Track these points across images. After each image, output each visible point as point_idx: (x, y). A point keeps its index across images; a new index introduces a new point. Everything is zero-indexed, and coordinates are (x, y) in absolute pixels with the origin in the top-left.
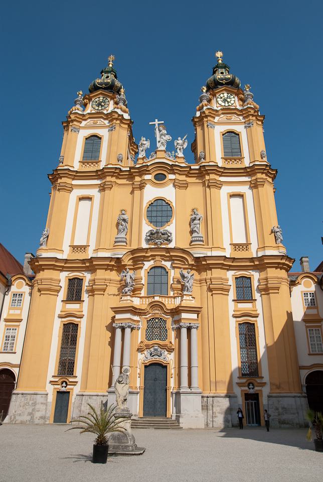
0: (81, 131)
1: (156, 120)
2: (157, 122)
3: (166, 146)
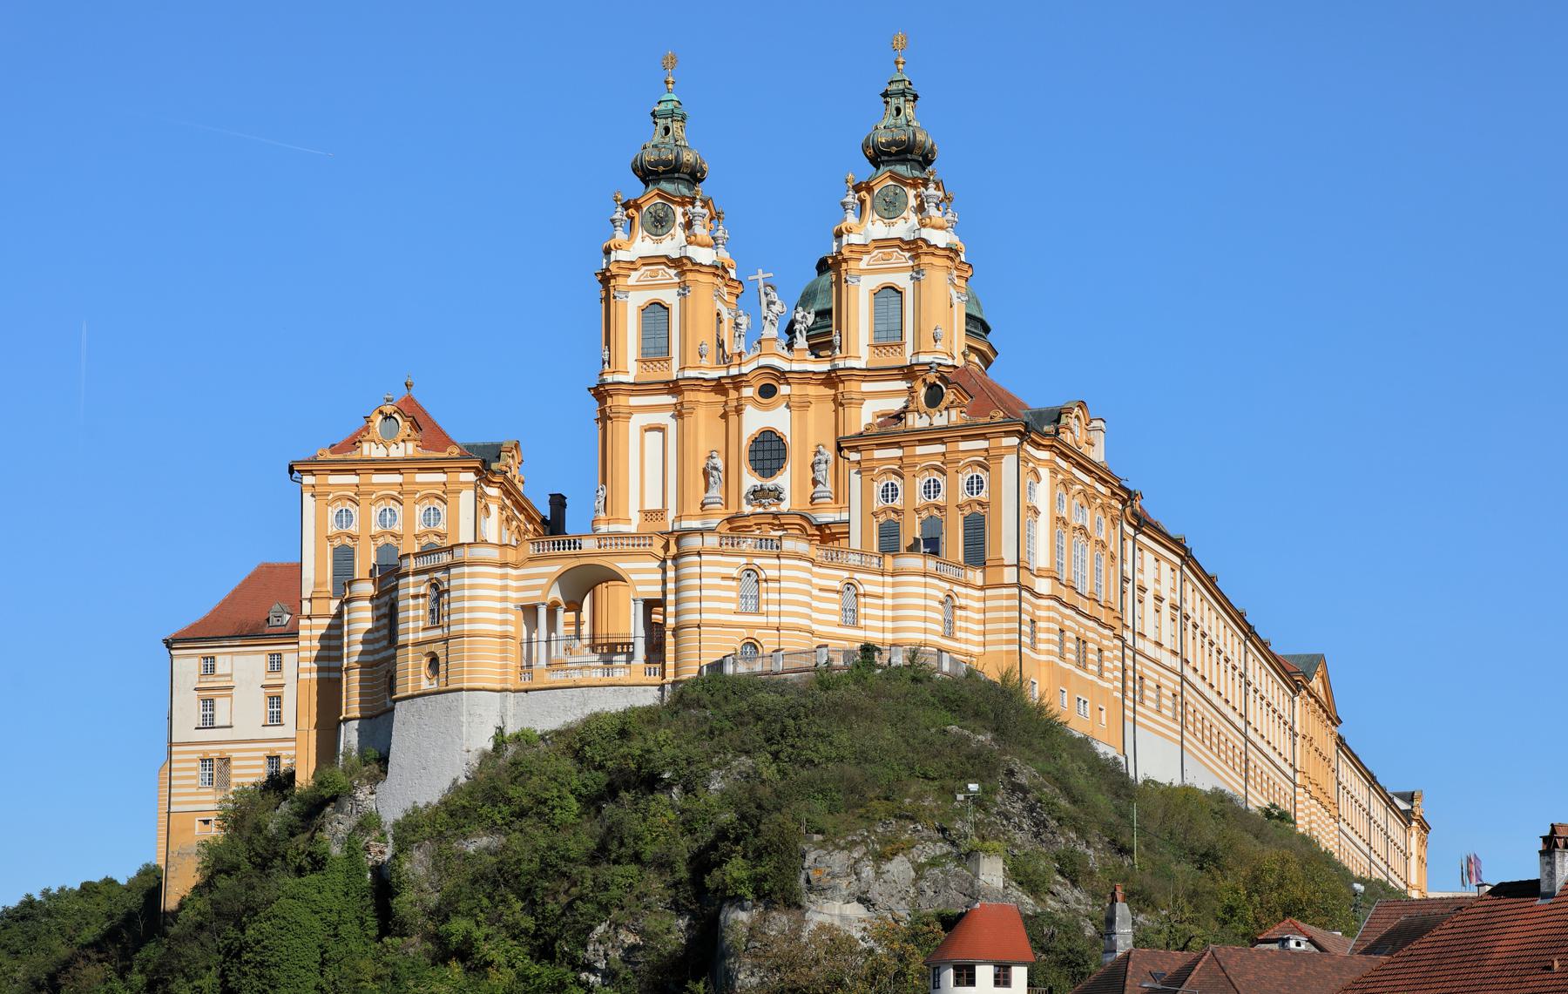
1: (760, 271)
2: (761, 275)
3: (777, 325)
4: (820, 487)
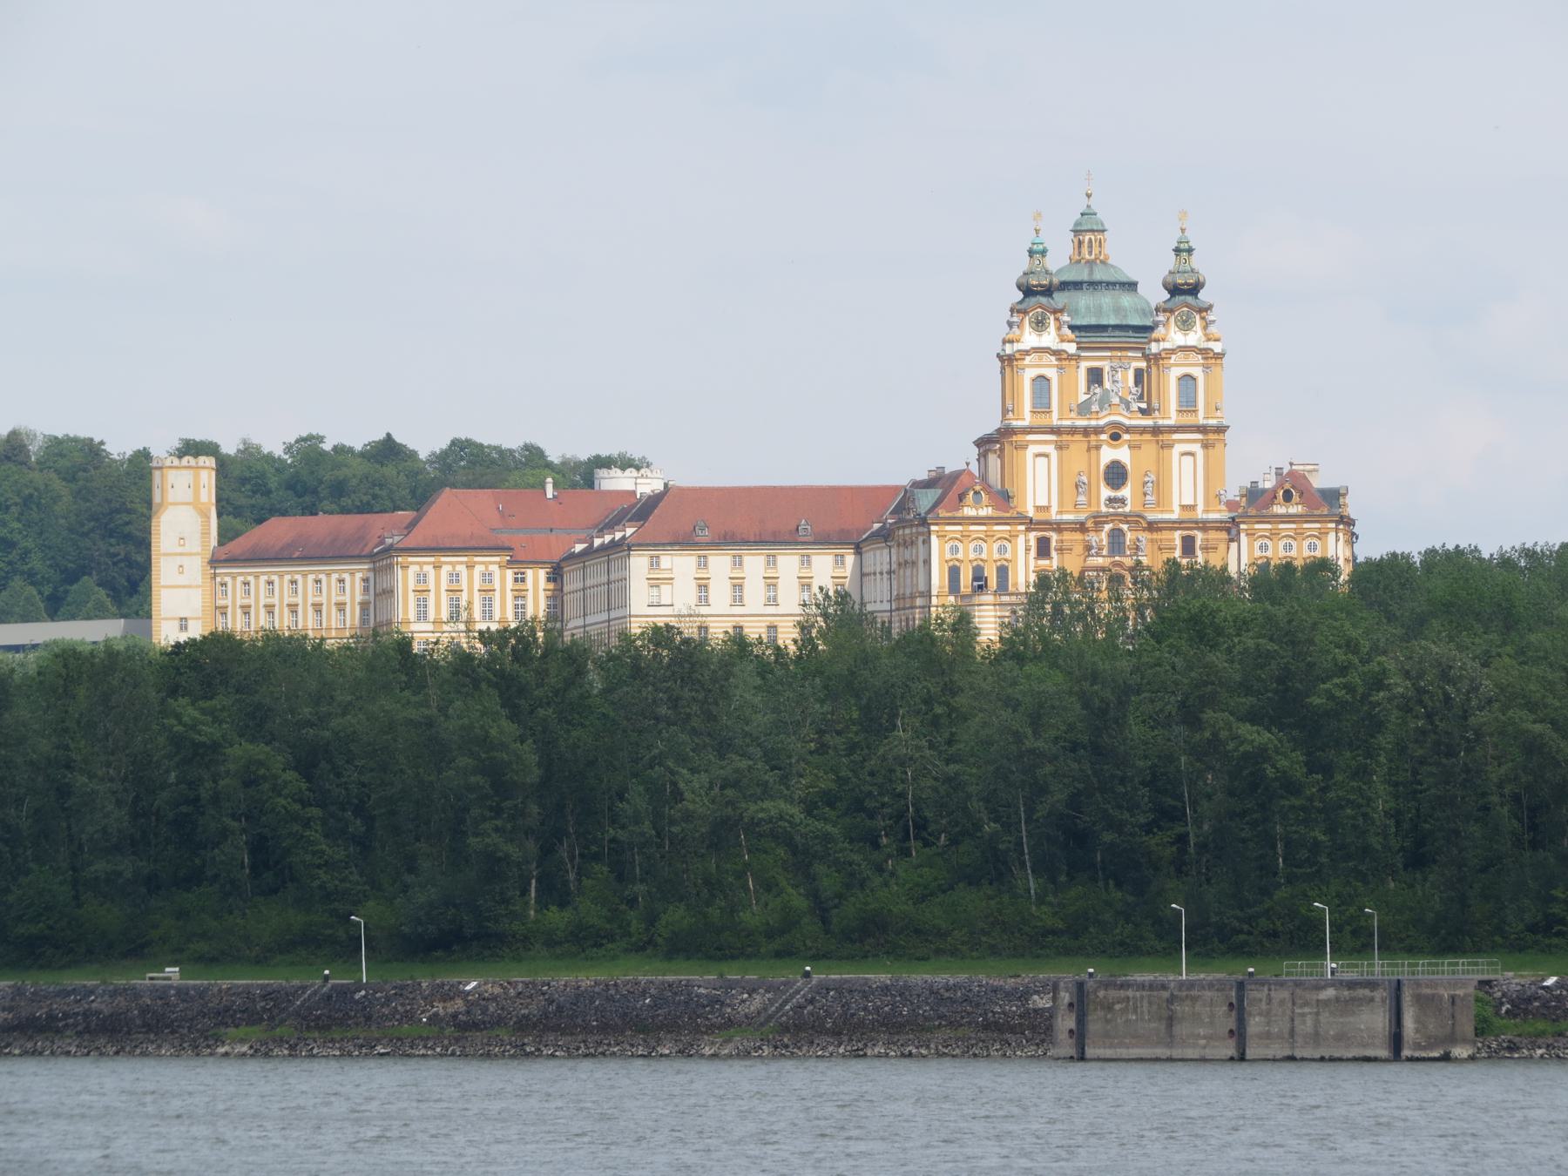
0: (1027, 369)
4: (1148, 497)
